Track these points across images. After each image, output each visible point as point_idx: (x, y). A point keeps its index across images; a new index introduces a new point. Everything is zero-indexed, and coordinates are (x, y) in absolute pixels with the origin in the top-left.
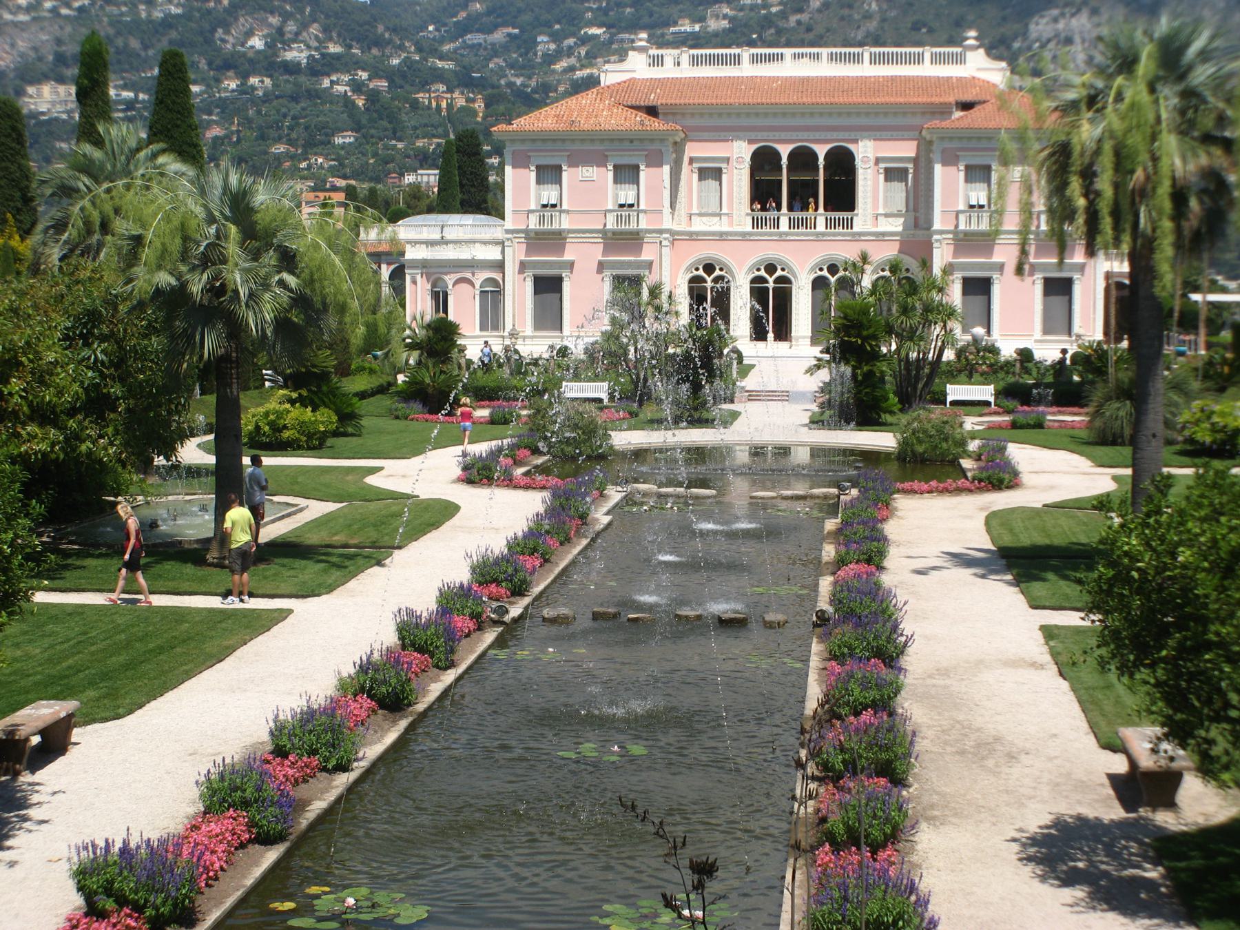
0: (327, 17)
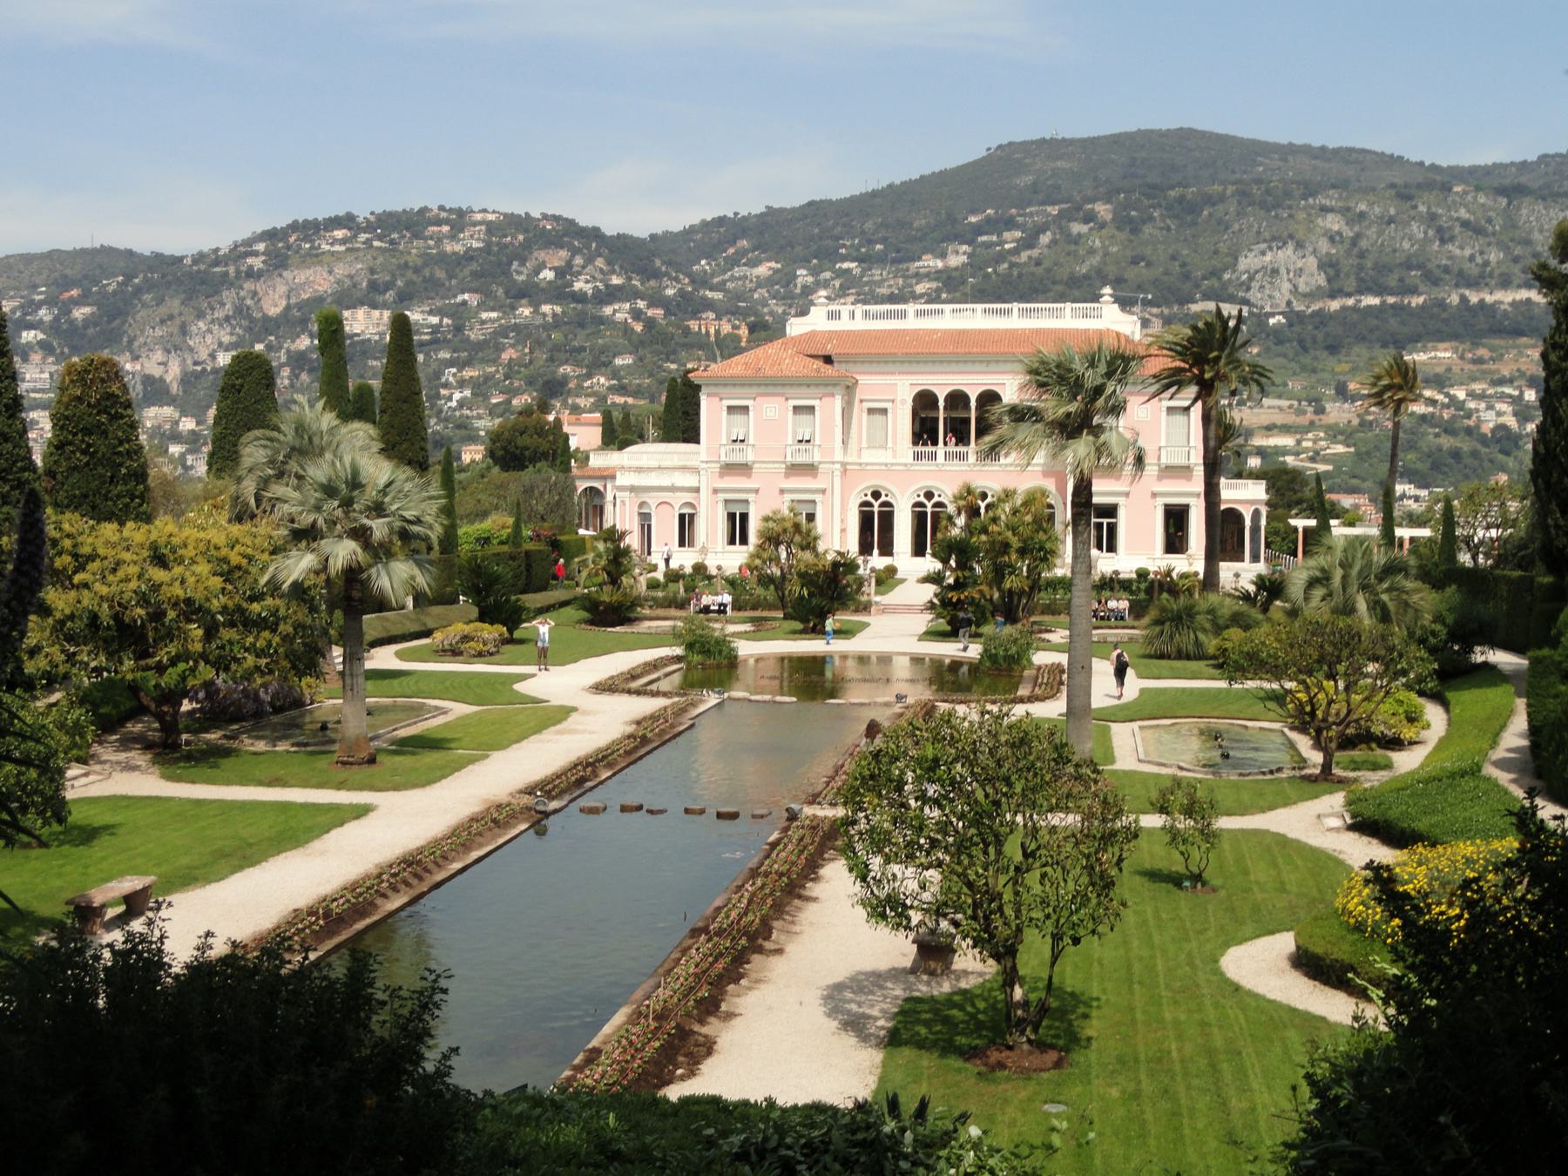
0: (611, 251)
